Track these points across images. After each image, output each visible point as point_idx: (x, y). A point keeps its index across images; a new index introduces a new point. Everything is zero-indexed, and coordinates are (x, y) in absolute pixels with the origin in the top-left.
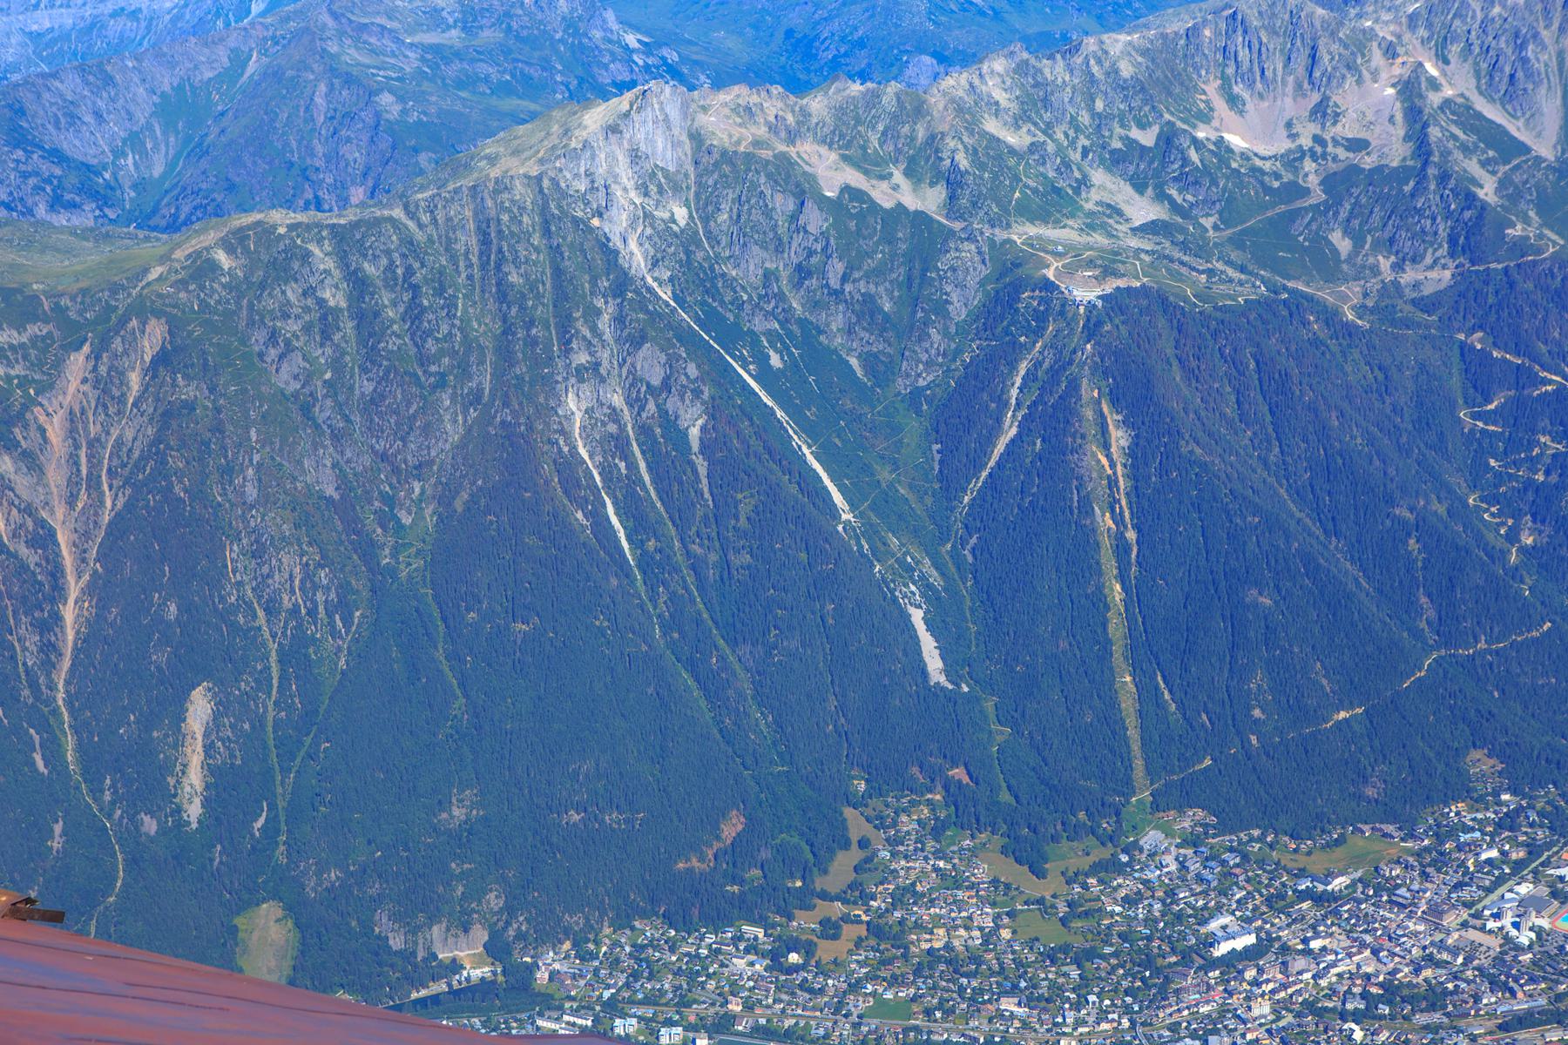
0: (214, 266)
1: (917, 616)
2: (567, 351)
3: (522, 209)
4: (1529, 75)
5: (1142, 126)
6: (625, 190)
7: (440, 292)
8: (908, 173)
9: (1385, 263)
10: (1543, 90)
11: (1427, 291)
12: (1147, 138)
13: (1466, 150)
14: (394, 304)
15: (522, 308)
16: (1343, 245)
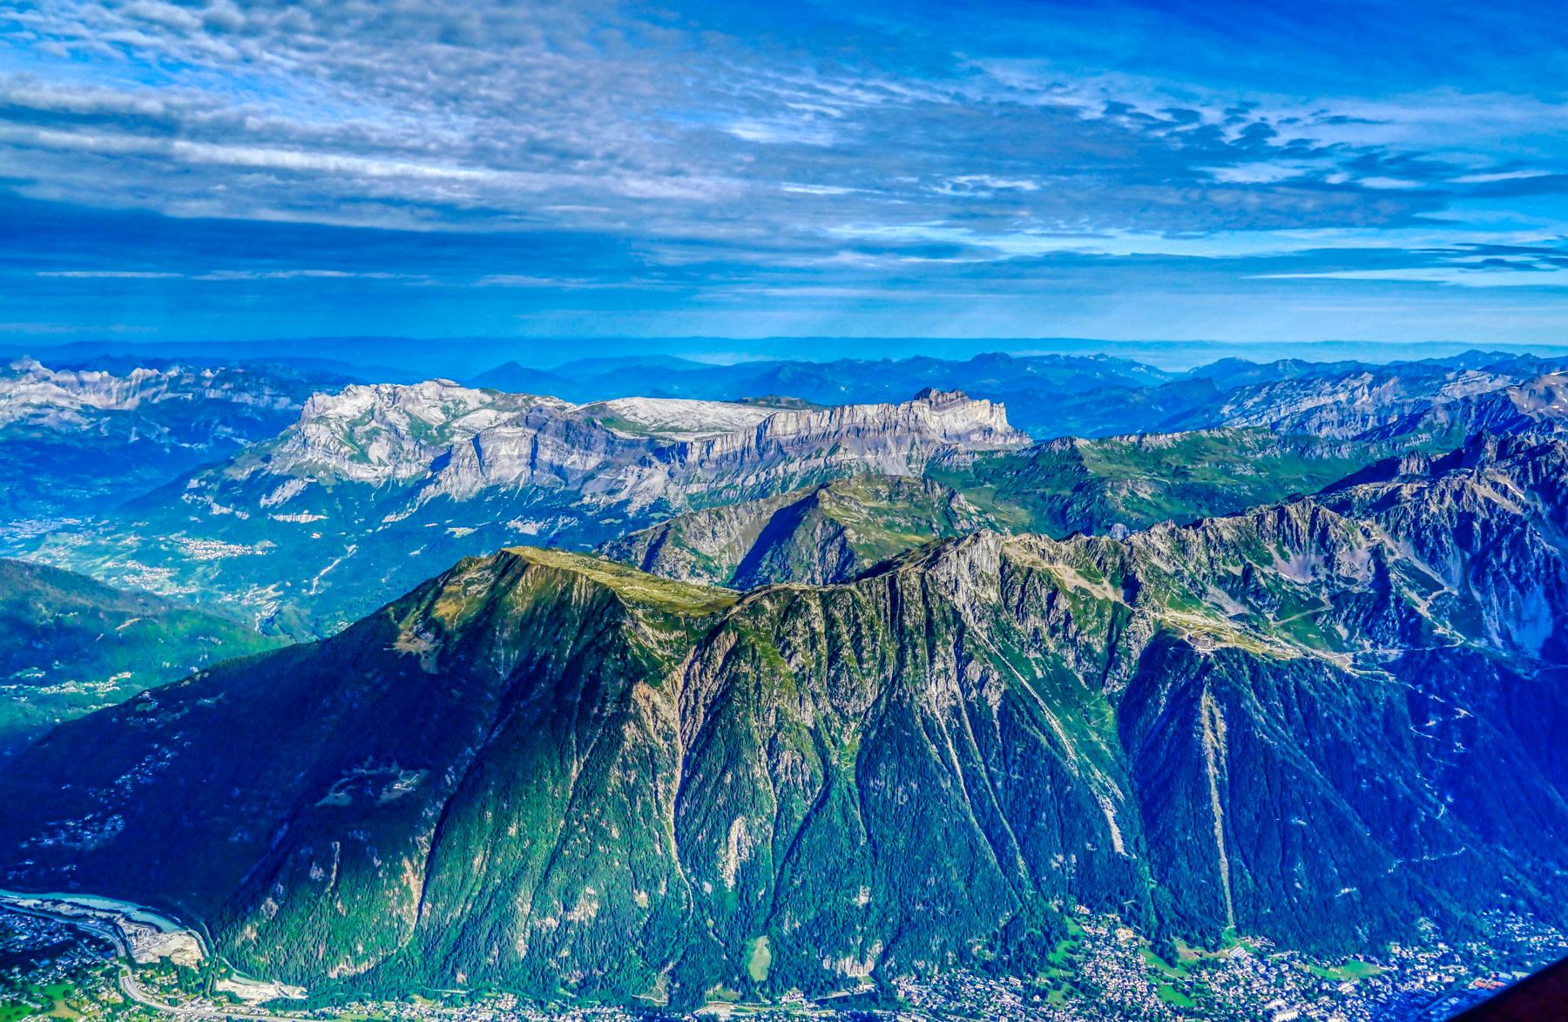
0: (763, 608)
1: (1110, 815)
2: (932, 662)
4: (1442, 550)
5: (1235, 565)
7: (871, 628)
8: (1111, 582)
9: (1367, 644)
10: (1451, 557)
11: (1391, 659)
12: (1237, 571)
13: (1411, 588)
16: (1344, 633)
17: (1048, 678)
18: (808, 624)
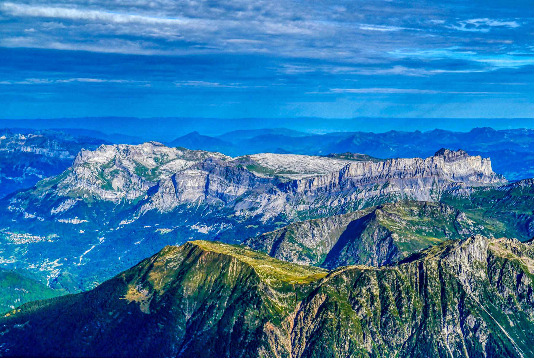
0: (342, 280)
2: (445, 315)
3: (434, 270)
6: (466, 266)
7: (407, 293)
14: (393, 295)
15: (432, 300)
17: (517, 326)
18: (369, 290)
